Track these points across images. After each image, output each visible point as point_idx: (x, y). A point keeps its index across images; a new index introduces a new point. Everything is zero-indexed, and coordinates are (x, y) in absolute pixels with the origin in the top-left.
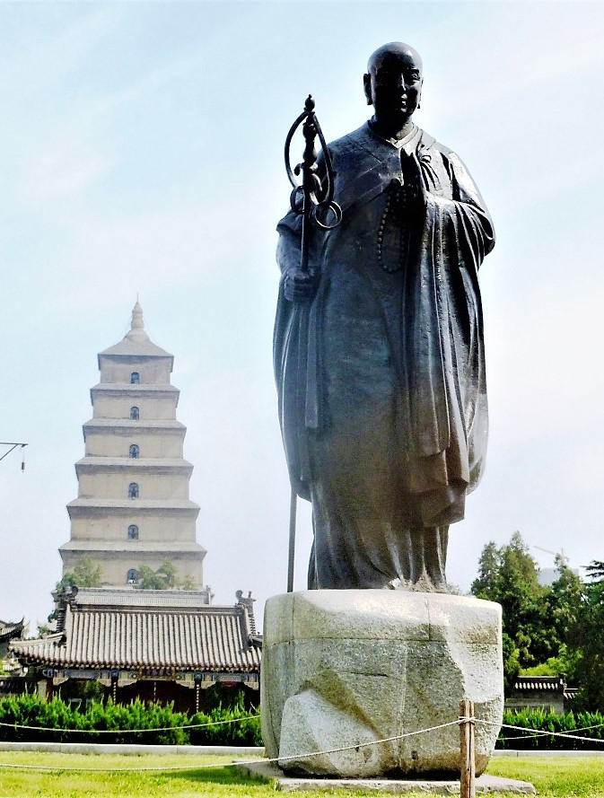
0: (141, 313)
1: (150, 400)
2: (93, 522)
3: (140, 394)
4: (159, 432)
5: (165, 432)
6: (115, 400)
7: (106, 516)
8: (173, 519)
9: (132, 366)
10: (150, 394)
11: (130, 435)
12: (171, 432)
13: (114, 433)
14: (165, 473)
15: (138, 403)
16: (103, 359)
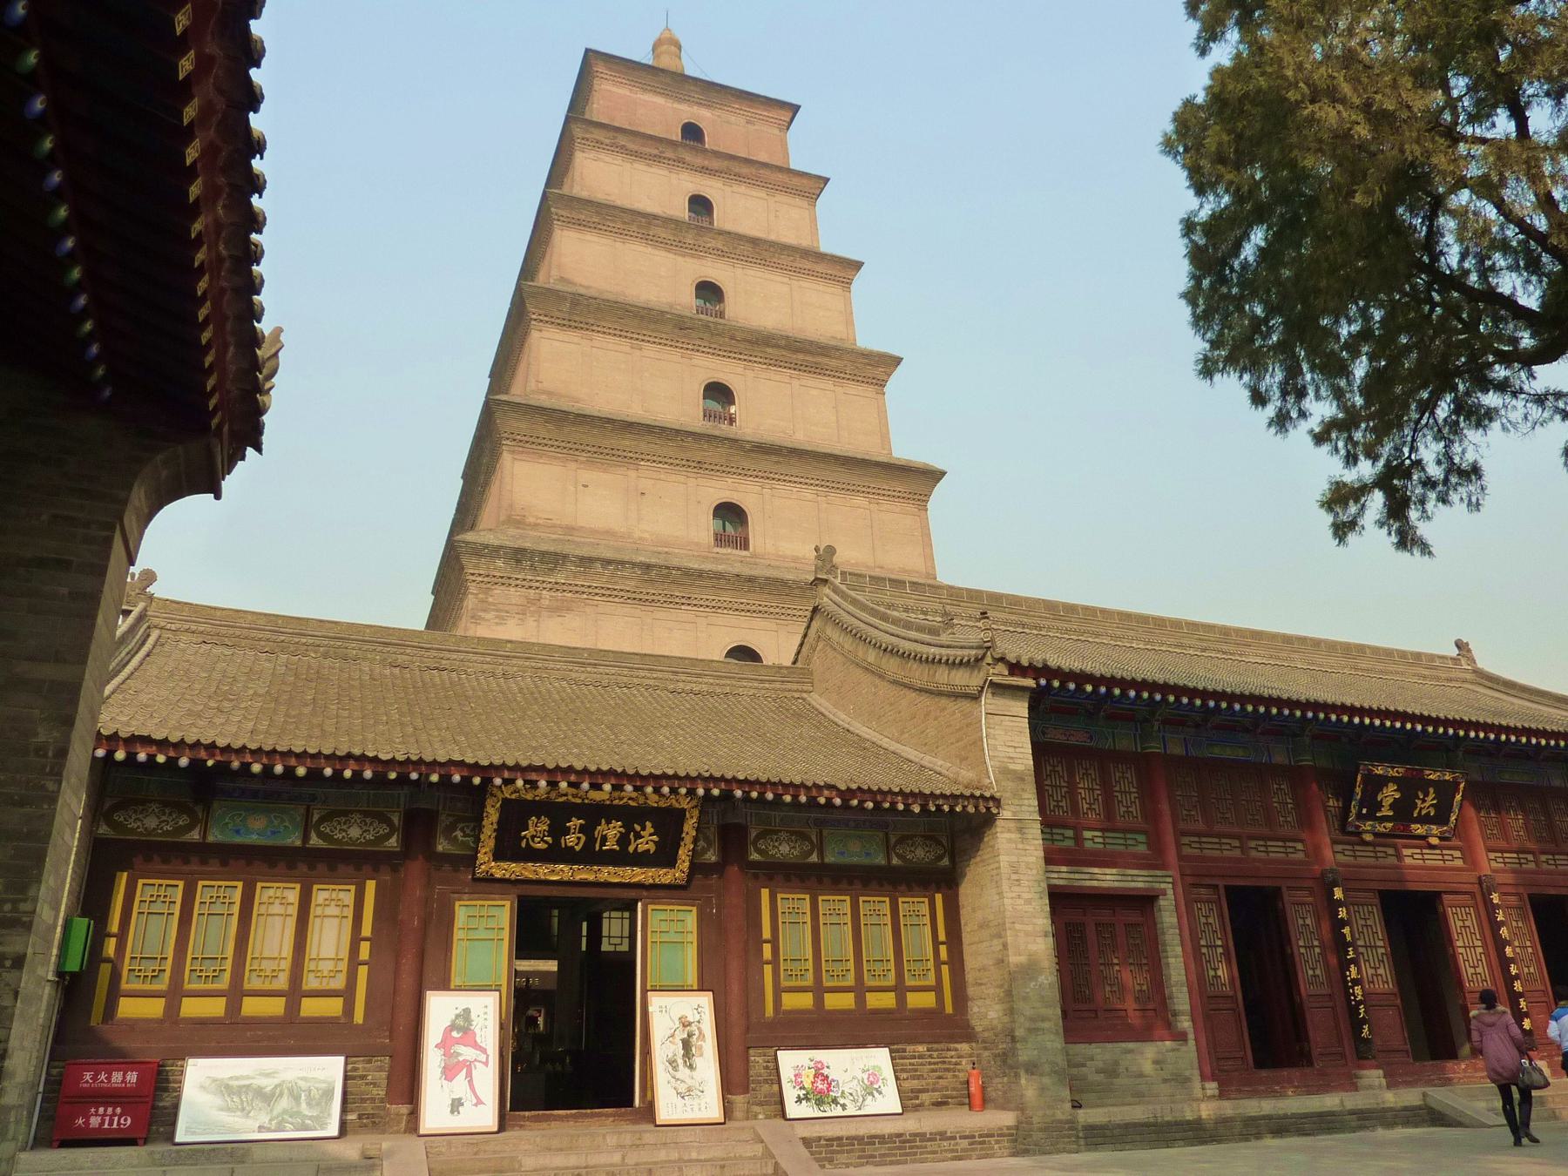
0: (680, 48)
1: (743, 189)
2: (587, 475)
3: (715, 164)
4: (785, 260)
5: (807, 265)
6: (640, 166)
7: (630, 460)
8: (860, 500)
9: (683, 107)
10: (745, 170)
11: (696, 251)
12: (820, 268)
13: (647, 239)
14: (817, 370)
15: (712, 188)
16: (599, 68)
